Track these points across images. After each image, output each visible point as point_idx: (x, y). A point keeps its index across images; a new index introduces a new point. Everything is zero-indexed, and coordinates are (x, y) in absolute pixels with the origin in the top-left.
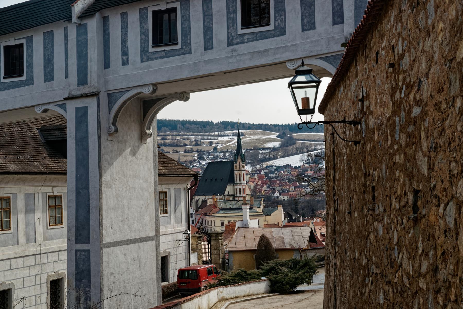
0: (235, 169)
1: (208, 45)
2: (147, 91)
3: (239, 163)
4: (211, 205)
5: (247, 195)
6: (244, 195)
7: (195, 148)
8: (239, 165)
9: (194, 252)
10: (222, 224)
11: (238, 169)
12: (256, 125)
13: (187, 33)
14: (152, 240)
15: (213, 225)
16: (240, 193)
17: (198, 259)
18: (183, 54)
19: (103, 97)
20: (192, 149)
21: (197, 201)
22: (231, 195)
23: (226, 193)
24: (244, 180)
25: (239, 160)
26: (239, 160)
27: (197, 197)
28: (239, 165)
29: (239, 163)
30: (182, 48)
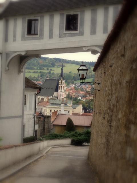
0: (59, 84)
1: (51, 36)
2: (23, 54)
4: (46, 101)
5: (65, 97)
6: (63, 97)
7: (39, 71)
9: (36, 125)
10: (51, 111)
12: (72, 61)
13: (42, 30)
14: (20, 117)
15: (46, 111)
16: (61, 96)
17: (39, 128)
18: (40, 39)
19: (4, 56)
20: (38, 71)
22: (56, 97)
23: (54, 96)
24: (63, 89)
26: (62, 79)
30: (39, 37)
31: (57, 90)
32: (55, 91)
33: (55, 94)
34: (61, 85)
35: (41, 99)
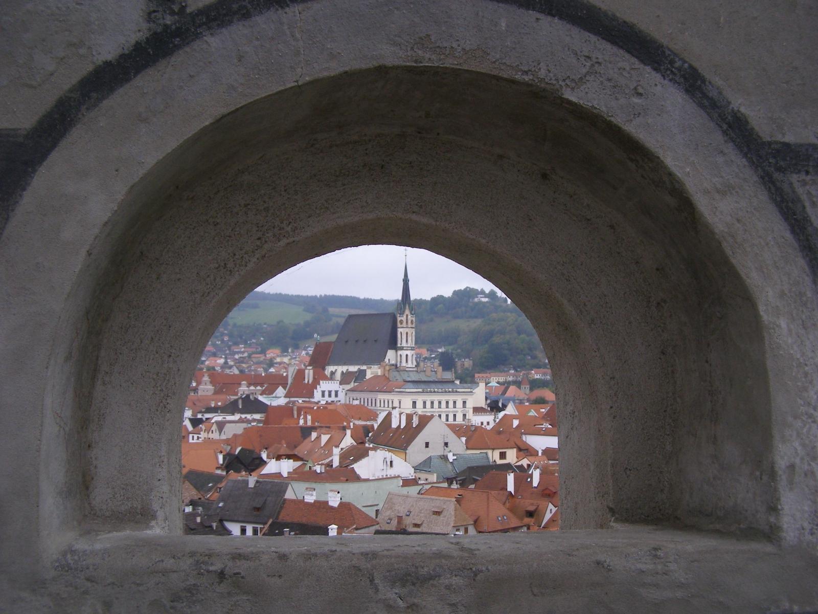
0: (399, 325)
3: (407, 316)
4: (376, 377)
8: (407, 319)
11: (404, 325)
12: (273, 295)
21: (333, 373)
22: (393, 365)
23: (387, 360)
25: (407, 312)
26: (407, 312)
27: (332, 367)
28: (407, 319)
29: (407, 316)
31: (393, 343)
32: (390, 349)
33: (391, 354)
34: (407, 330)
35: (343, 372)
